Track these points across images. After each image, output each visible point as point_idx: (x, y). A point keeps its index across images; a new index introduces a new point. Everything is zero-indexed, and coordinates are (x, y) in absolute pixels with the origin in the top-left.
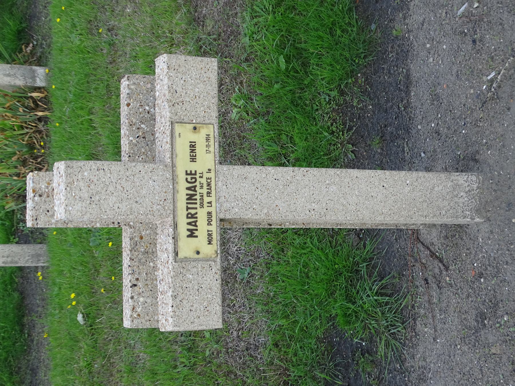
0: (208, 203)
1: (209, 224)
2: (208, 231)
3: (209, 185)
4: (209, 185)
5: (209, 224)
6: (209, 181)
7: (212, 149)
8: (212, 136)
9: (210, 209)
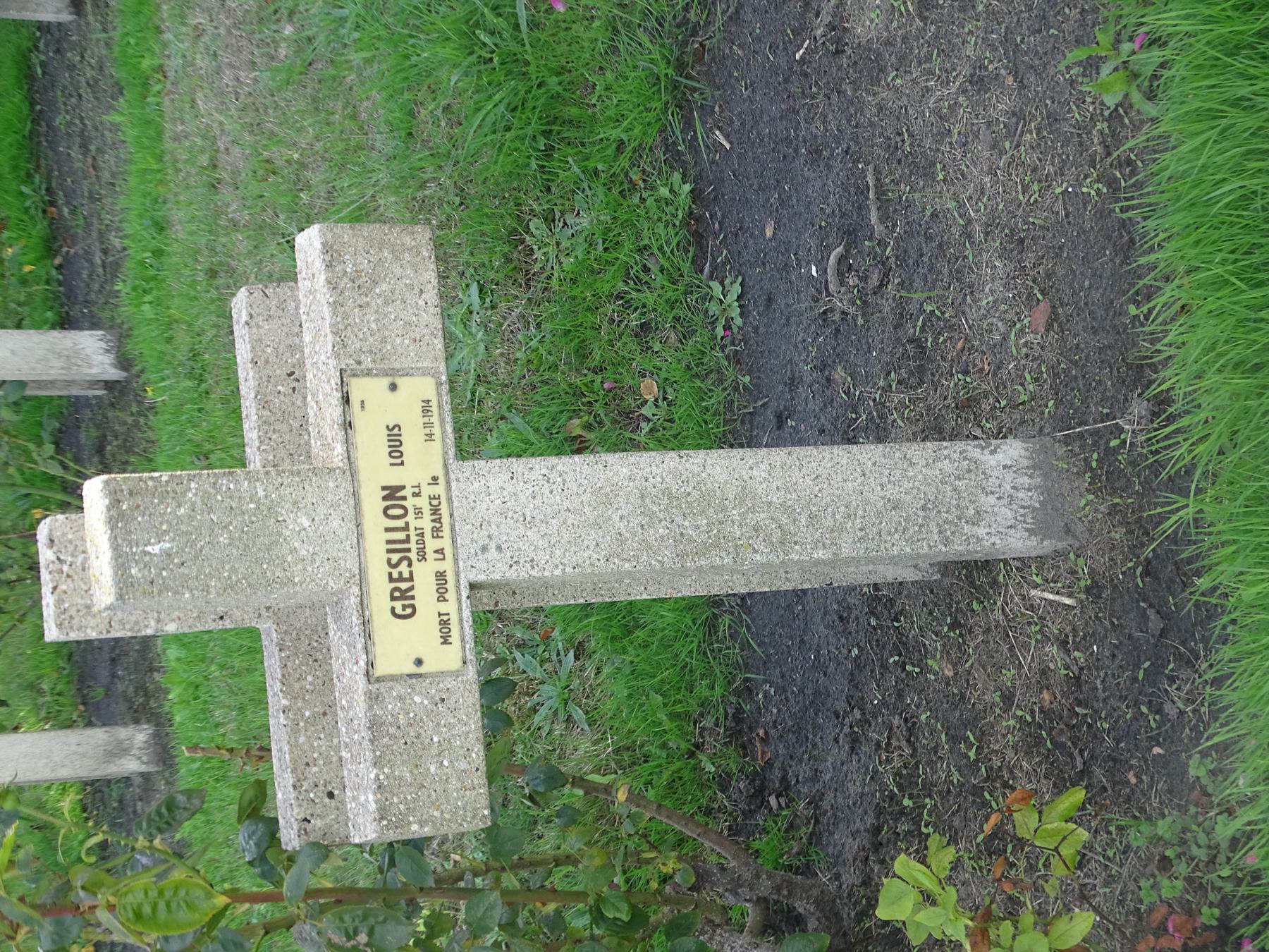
0: (436, 552)
1: (442, 598)
2: (440, 615)
3: (435, 511)
4: (435, 511)
5: (442, 598)
6: (435, 502)
7: (437, 430)
8: (434, 404)
9: (441, 566)
